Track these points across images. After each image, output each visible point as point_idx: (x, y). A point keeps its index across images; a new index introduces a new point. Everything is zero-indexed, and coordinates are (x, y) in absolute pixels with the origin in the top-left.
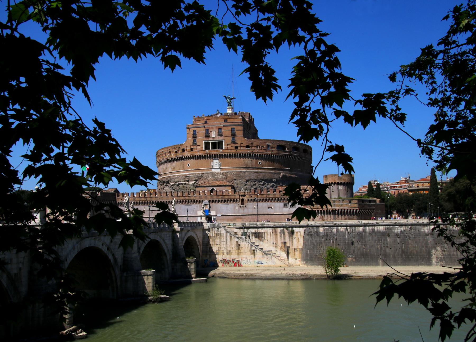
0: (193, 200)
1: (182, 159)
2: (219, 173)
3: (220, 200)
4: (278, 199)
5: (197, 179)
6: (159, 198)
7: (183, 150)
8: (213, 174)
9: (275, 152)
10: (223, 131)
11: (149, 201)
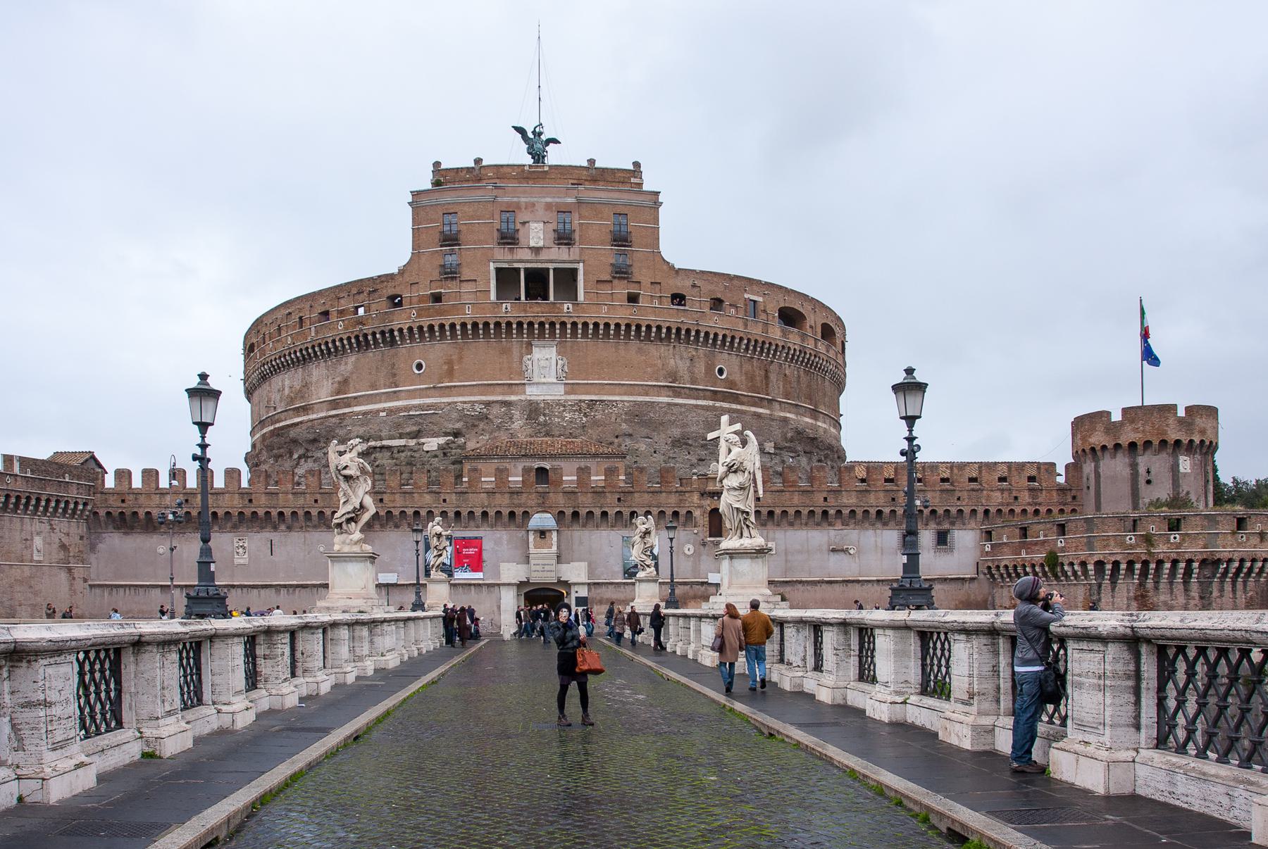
1: (389, 338)
4: (879, 513)
5: (458, 425)
8: (533, 410)
9: (776, 332)
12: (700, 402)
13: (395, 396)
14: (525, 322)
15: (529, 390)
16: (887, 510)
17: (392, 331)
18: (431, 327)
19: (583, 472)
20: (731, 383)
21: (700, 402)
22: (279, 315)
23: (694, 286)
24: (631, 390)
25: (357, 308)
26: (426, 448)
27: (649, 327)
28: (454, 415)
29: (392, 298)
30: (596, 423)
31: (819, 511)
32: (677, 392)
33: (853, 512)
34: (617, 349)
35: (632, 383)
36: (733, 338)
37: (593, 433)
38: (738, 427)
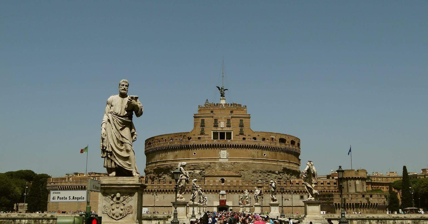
0: (209, 190)
2: (227, 163)
3: (238, 190)
4: (295, 191)
5: (204, 168)
8: (221, 164)
10: (231, 121)
11: (162, 190)
12: (260, 162)
15: (220, 160)
16: (297, 191)
18: (198, 145)
20: (266, 157)
21: (260, 162)
29: (188, 138)
30: (235, 167)
35: (243, 158)
37: (235, 170)
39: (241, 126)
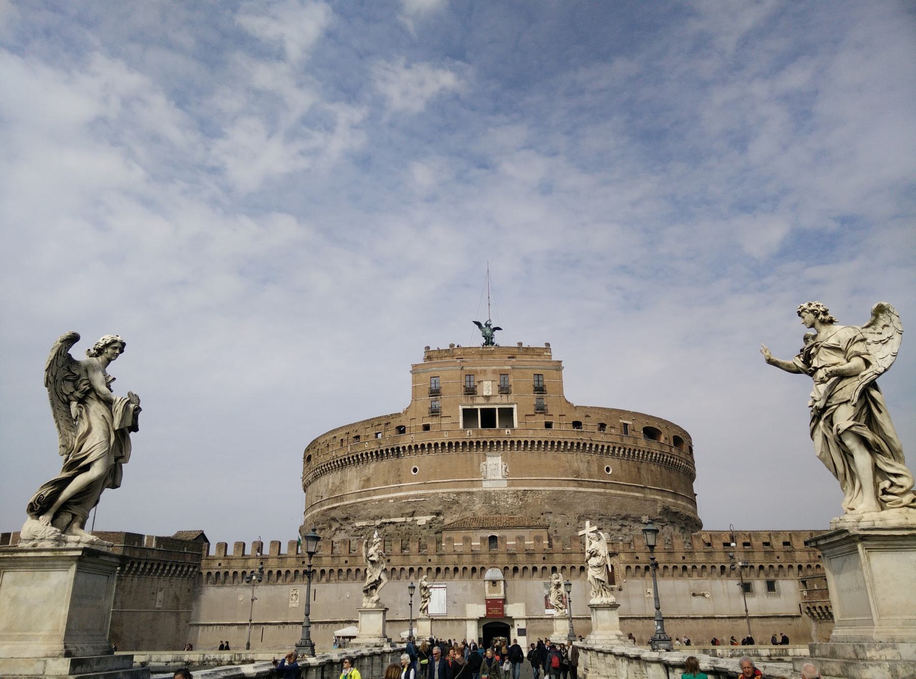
0: (452, 568)
1: (397, 452)
3: (539, 567)
5: (440, 508)
6: (343, 560)
7: (401, 430)
8: (488, 497)
9: (643, 443)
10: (511, 380)
12: (596, 490)
13: (399, 489)
14: (482, 441)
15: (485, 484)
16: (728, 566)
17: (398, 448)
18: (423, 445)
19: (520, 539)
21: (596, 490)
22: (328, 438)
23: (587, 416)
24: (550, 482)
25: (377, 434)
26: (419, 523)
27: (559, 443)
28: (437, 501)
29: (399, 428)
31: (680, 566)
32: (580, 483)
33: (704, 567)
34: (540, 457)
35: (549, 478)
36: (614, 448)
38: (595, 528)
39: (540, 390)
